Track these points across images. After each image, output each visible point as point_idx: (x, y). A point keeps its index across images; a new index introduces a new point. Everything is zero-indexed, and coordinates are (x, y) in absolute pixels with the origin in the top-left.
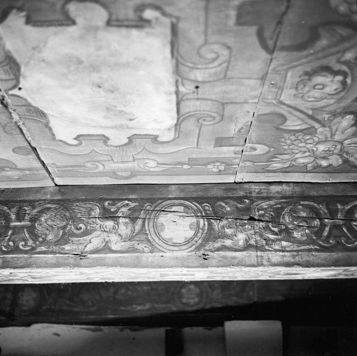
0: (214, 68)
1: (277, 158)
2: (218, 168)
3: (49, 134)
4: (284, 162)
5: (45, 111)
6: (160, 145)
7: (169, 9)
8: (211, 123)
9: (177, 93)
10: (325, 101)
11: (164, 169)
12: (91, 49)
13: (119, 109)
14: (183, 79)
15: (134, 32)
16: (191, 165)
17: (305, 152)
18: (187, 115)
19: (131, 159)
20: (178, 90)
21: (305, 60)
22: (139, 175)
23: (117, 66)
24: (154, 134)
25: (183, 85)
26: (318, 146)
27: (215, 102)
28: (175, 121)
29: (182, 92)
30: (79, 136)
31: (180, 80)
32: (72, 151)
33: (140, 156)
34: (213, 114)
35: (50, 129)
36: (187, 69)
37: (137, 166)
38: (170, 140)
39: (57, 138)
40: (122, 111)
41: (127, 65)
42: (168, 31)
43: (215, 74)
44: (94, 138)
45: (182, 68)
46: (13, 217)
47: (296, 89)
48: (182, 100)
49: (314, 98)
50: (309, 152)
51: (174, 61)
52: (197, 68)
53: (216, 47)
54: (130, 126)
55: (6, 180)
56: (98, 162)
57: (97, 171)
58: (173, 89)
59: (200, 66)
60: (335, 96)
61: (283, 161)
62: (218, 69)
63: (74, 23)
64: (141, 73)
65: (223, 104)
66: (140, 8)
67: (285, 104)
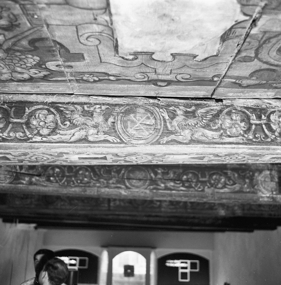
0: (85, 32)
7: (121, 59)
9: (110, 14)
14: (108, 26)
15: (139, 50)
20: (110, 18)
21: (26, 34)
23: (154, 34)
25: (107, 21)
29: (107, 16)
31: (110, 25)
36: (105, 32)
41: (148, 34)
43: (84, 28)
45: (110, 33)
47: (14, 15)
48: (106, 9)
51: (115, 37)
52: (99, 32)
53: (89, 44)
58: (114, 18)
59: (97, 34)
62: (83, 32)
63: (172, 54)
64: (138, 30)
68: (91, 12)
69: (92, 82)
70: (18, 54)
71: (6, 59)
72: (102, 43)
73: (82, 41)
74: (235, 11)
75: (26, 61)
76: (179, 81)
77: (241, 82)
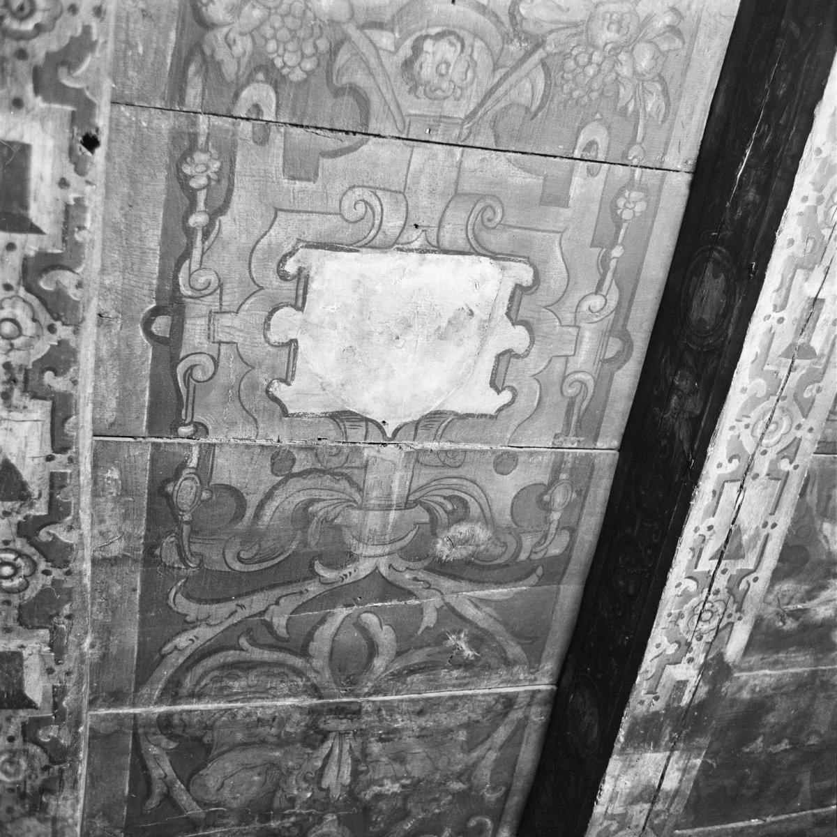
1: (626, 108)
2: (635, 203)
3: (481, 420)
4: (643, 92)
5: (432, 409)
6: (543, 286)
8: (499, 211)
9: (422, 251)
10: (475, 55)
11: (614, 286)
12: (334, 333)
13: (444, 325)
14: (395, 243)
15: (313, 286)
16: (613, 244)
17: (617, 62)
18: (473, 242)
19: (573, 331)
20: (416, 250)
22: (624, 325)
24: (510, 289)
26: (601, 43)
27: (452, 205)
28: (487, 259)
30: (493, 384)
32: (526, 403)
33: (568, 317)
34: (478, 207)
35: (469, 415)
36: (380, 236)
37: (593, 326)
38: (531, 270)
39: (493, 413)
40: (449, 322)
42: (316, 253)
44: (502, 369)
45: (377, 242)
46: (629, 530)
48: (438, 247)
49: (467, 70)
50: (617, 55)
51: (364, 250)
53: (346, 203)
54: (486, 317)
55: (577, 511)
56: (564, 378)
57: (591, 385)
58: (414, 256)
59: (377, 222)
60: (467, 43)
61: (640, 95)
64: (379, 288)
65: (457, 194)
66: (284, 276)
67: (474, 112)
68: (435, 223)
69: (179, 170)
70: (323, 45)
71: (307, 7)
72: (345, 224)
73: (358, 191)
74: (405, 416)
75: (290, 47)
76: (174, 361)
77: (186, 479)
